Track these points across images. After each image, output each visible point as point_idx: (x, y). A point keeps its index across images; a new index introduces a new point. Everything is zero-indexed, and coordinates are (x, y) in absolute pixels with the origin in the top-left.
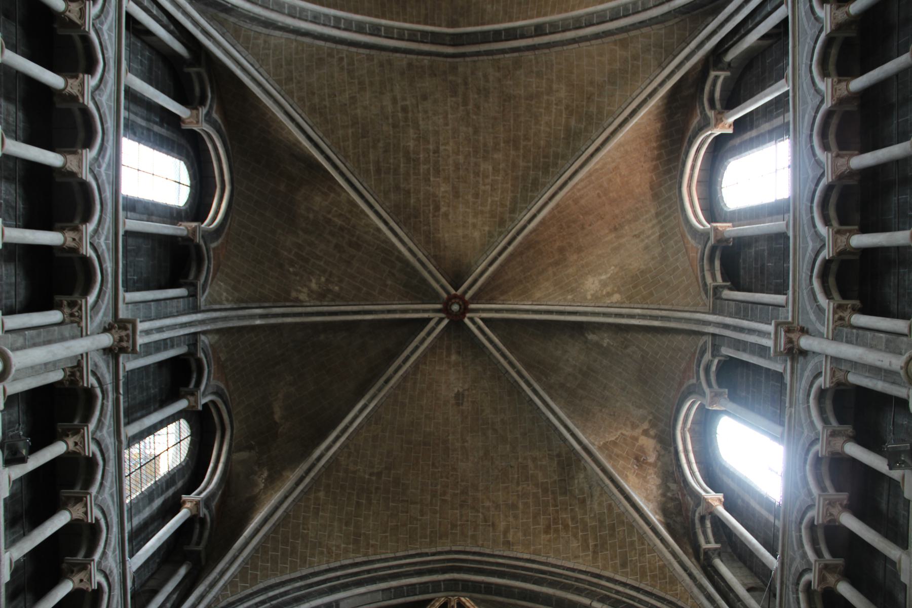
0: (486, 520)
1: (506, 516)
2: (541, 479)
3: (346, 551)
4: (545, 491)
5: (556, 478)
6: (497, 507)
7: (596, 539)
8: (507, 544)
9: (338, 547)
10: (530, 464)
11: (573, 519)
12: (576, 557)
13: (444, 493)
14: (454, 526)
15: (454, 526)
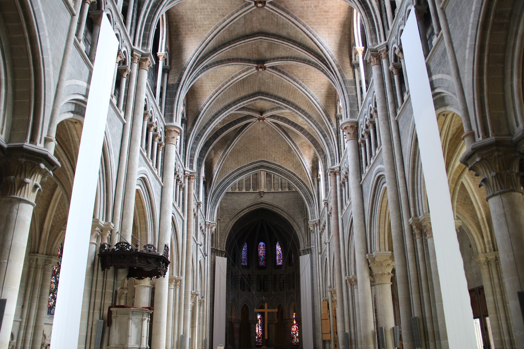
0: (269, 154)
1: (275, 154)
2: (284, 148)
3: (236, 166)
4: (285, 151)
5: (287, 149)
6: (273, 152)
7: (295, 166)
8: (275, 160)
9: (234, 166)
10: (281, 145)
11: (291, 159)
12: (291, 168)
13: (259, 148)
14: (261, 155)
15: (261, 155)
